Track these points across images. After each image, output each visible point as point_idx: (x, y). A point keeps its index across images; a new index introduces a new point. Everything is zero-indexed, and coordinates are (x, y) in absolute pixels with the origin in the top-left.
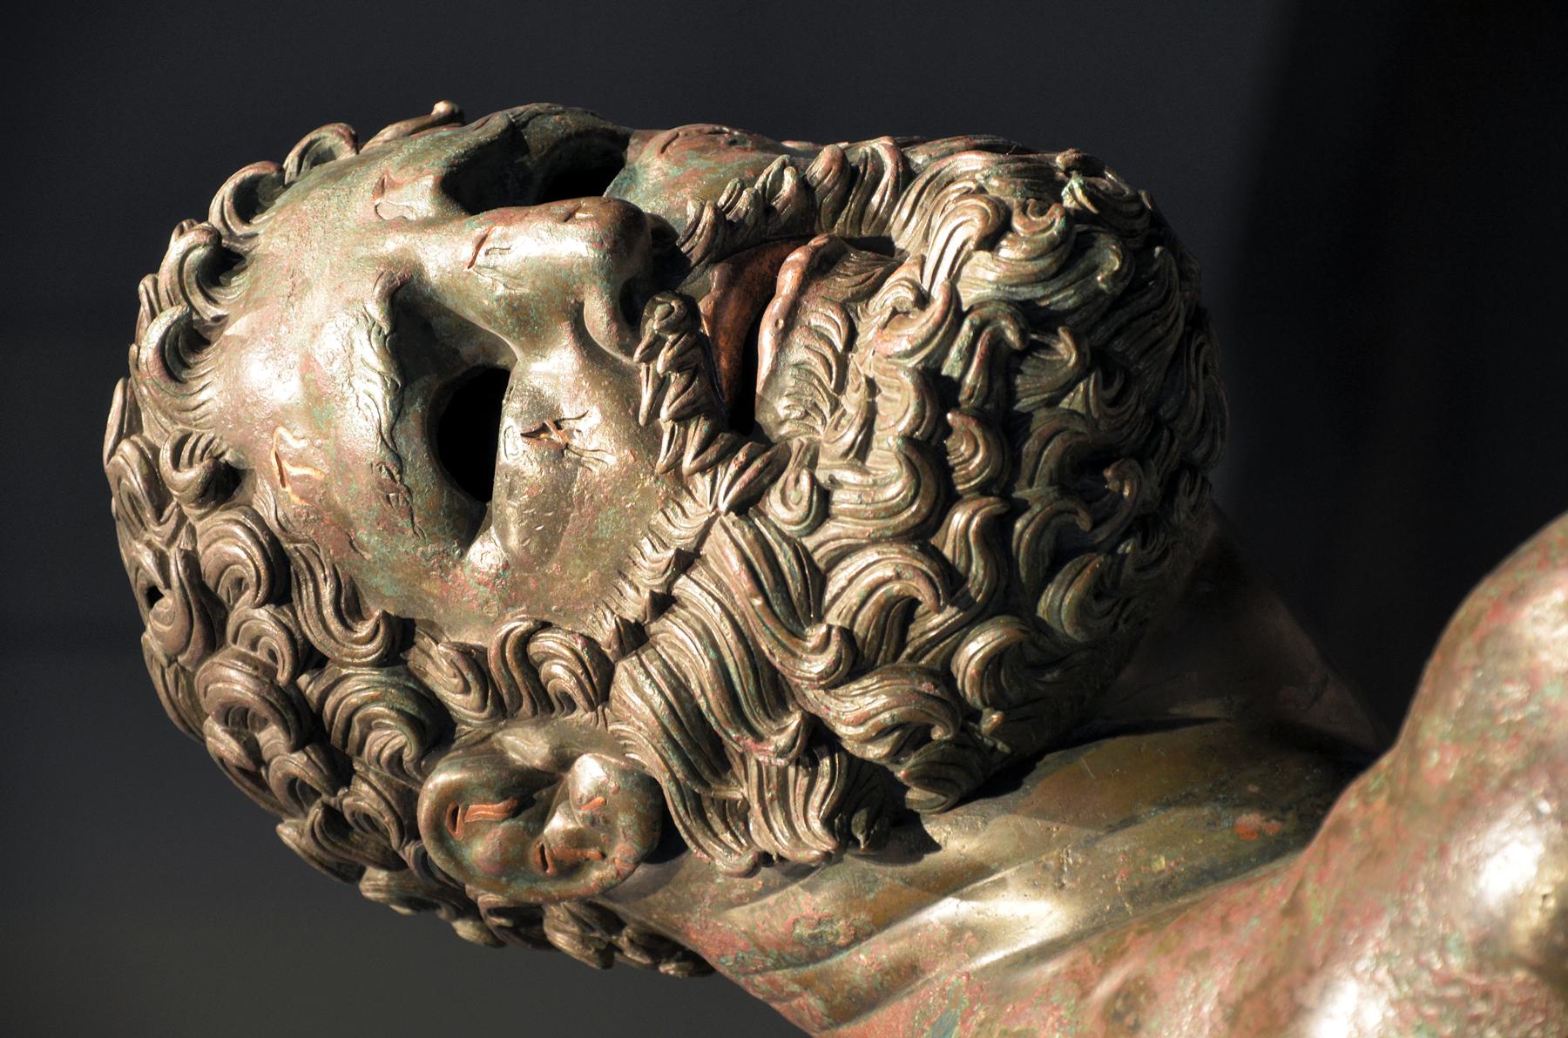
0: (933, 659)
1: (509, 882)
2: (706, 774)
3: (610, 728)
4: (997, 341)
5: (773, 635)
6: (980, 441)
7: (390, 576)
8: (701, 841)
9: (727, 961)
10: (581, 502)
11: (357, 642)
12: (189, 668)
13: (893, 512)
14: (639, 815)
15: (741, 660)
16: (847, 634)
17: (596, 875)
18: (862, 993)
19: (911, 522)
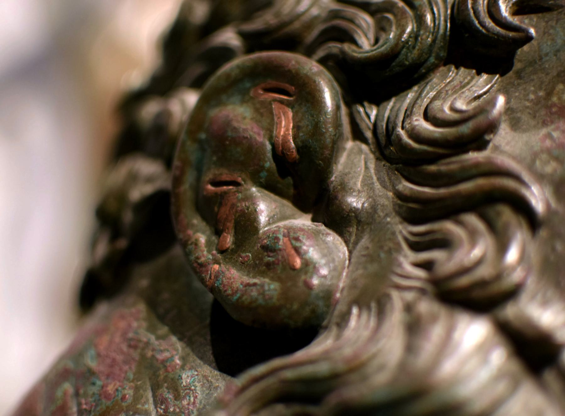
1: (200, 142)
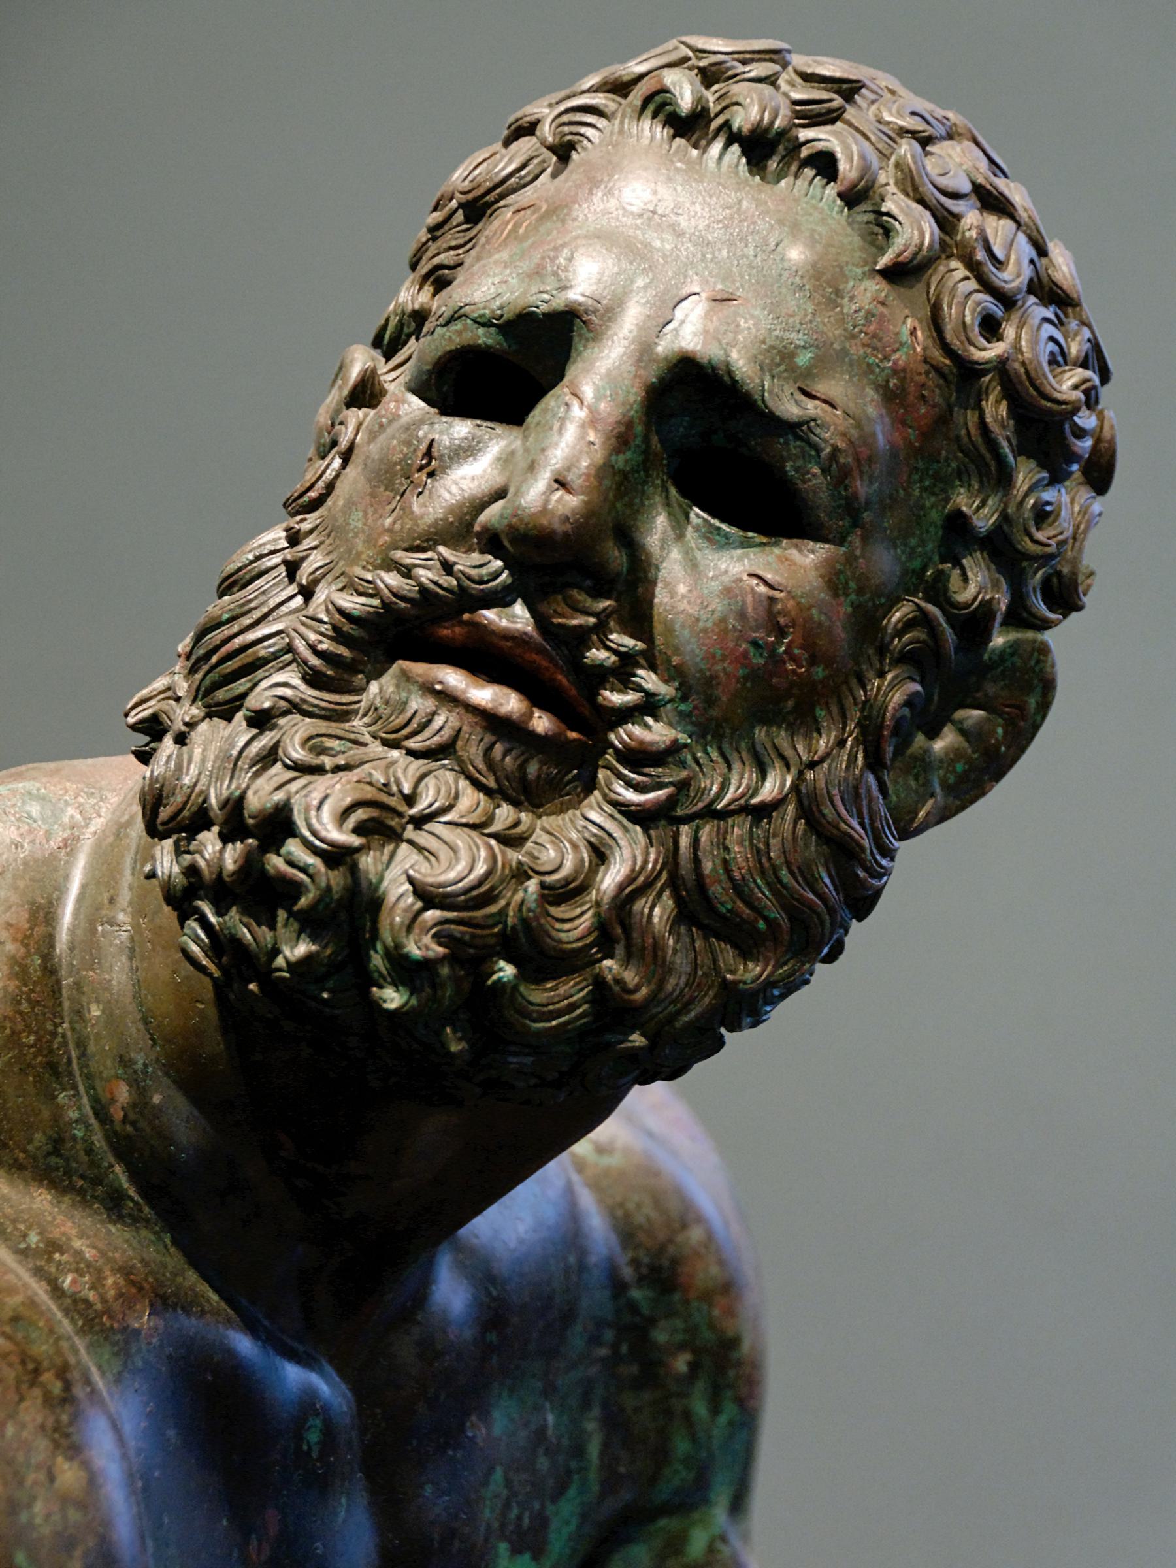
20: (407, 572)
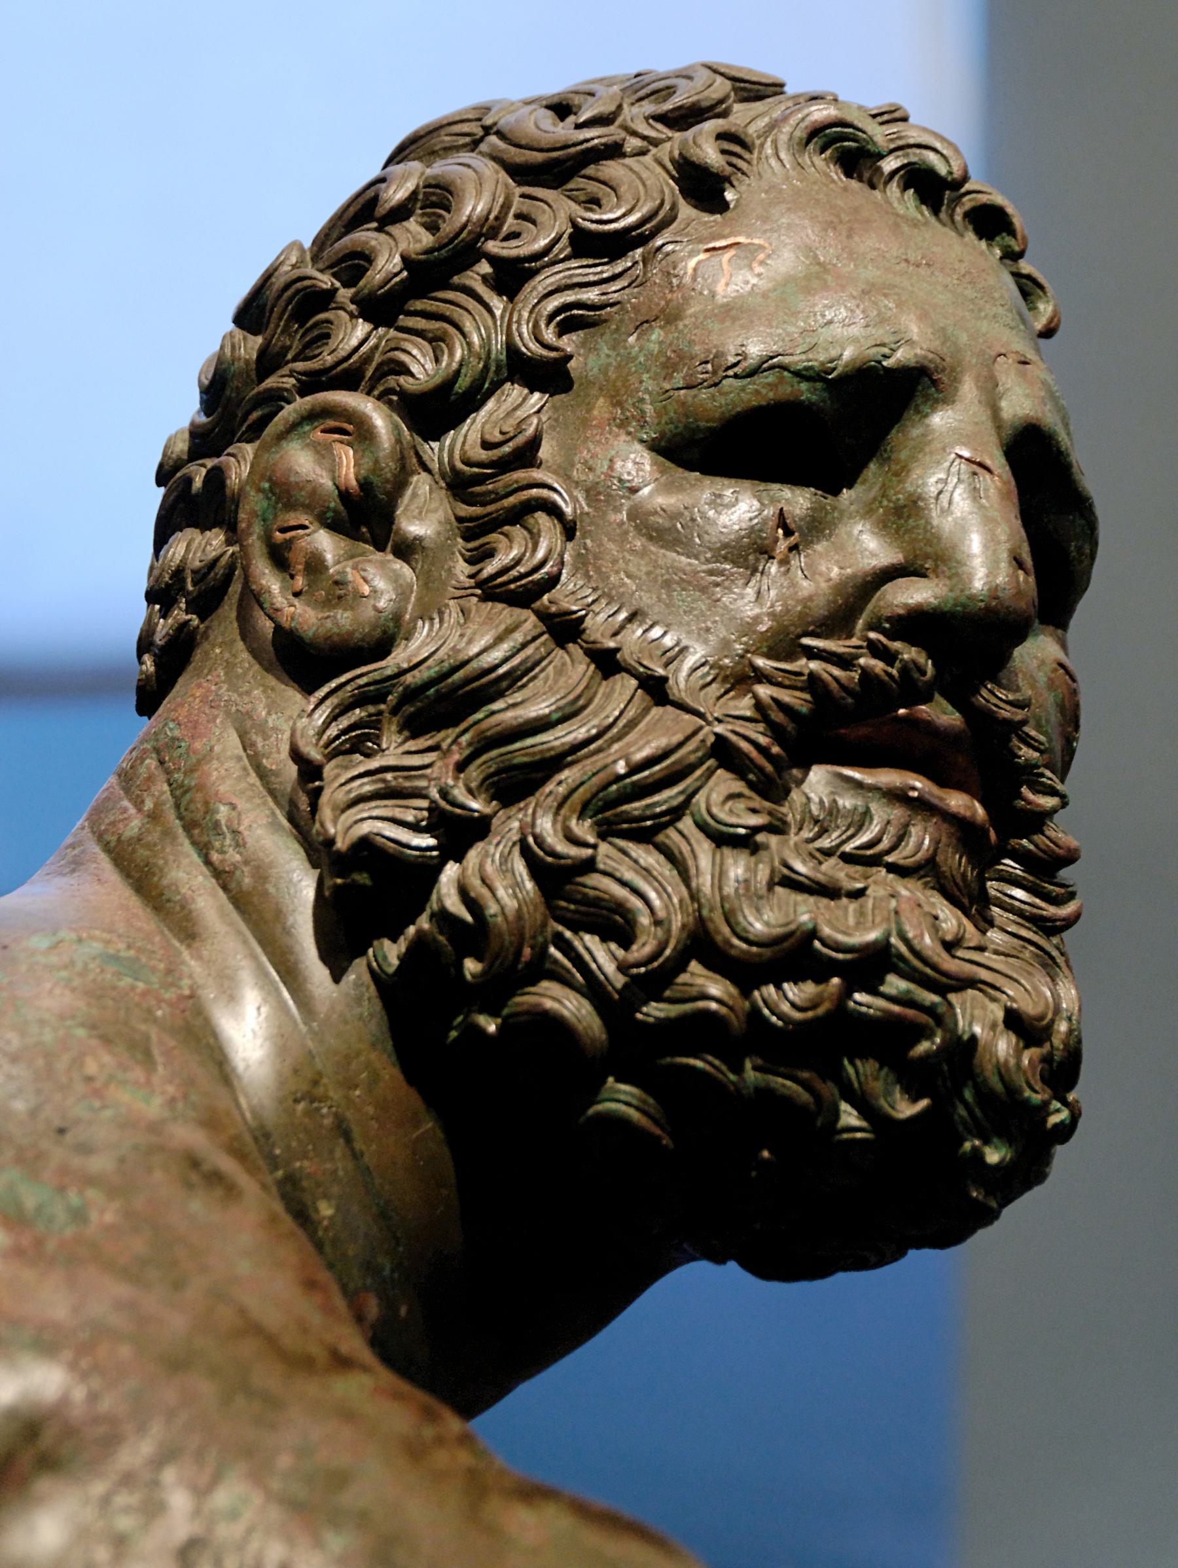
0: (556, 961)
2: (409, 709)
3: (452, 603)
4: (921, 1033)
5: (582, 783)
6: (810, 1014)
7: (610, 364)
8: (328, 702)
9: (171, 730)
10: (711, 573)
11: (536, 325)
12: (483, 147)
13: (729, 918)
14: (351, 634)
15: (552, 749)
16: (589, 865)
17: (271, 582)
18: (156, 879)
19: (719, 939)
20: (845, 662)
